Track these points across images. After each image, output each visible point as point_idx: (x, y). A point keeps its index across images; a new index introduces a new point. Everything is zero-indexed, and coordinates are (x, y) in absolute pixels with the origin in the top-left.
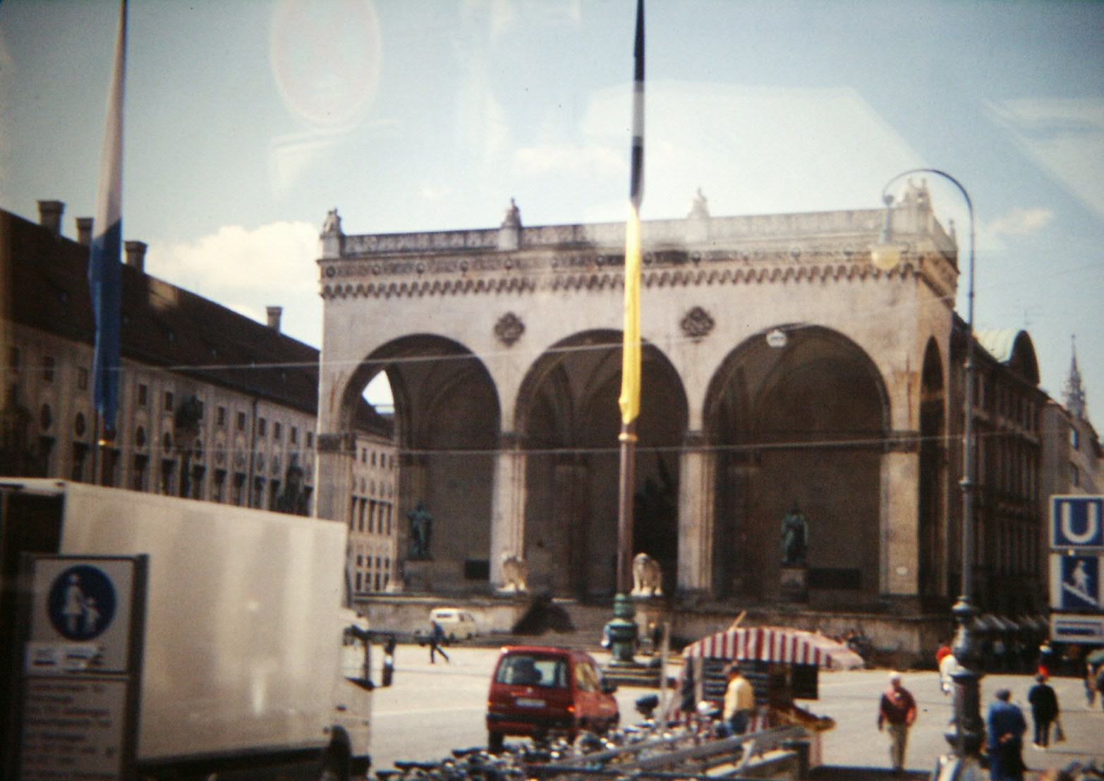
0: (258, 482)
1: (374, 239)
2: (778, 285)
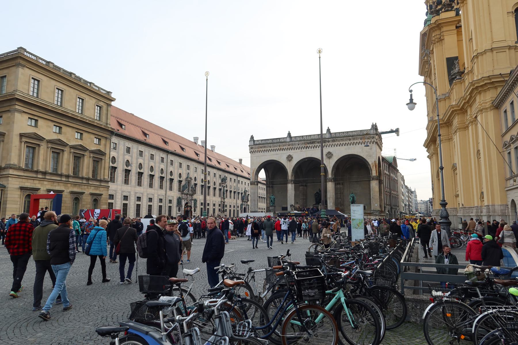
0: (239, 193)
2: (346, 146)
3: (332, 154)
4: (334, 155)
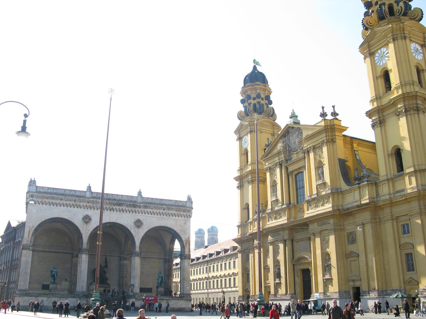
1: (47, 188)
2: (159, 216)
3: (142, 223)
4: (144, 224)
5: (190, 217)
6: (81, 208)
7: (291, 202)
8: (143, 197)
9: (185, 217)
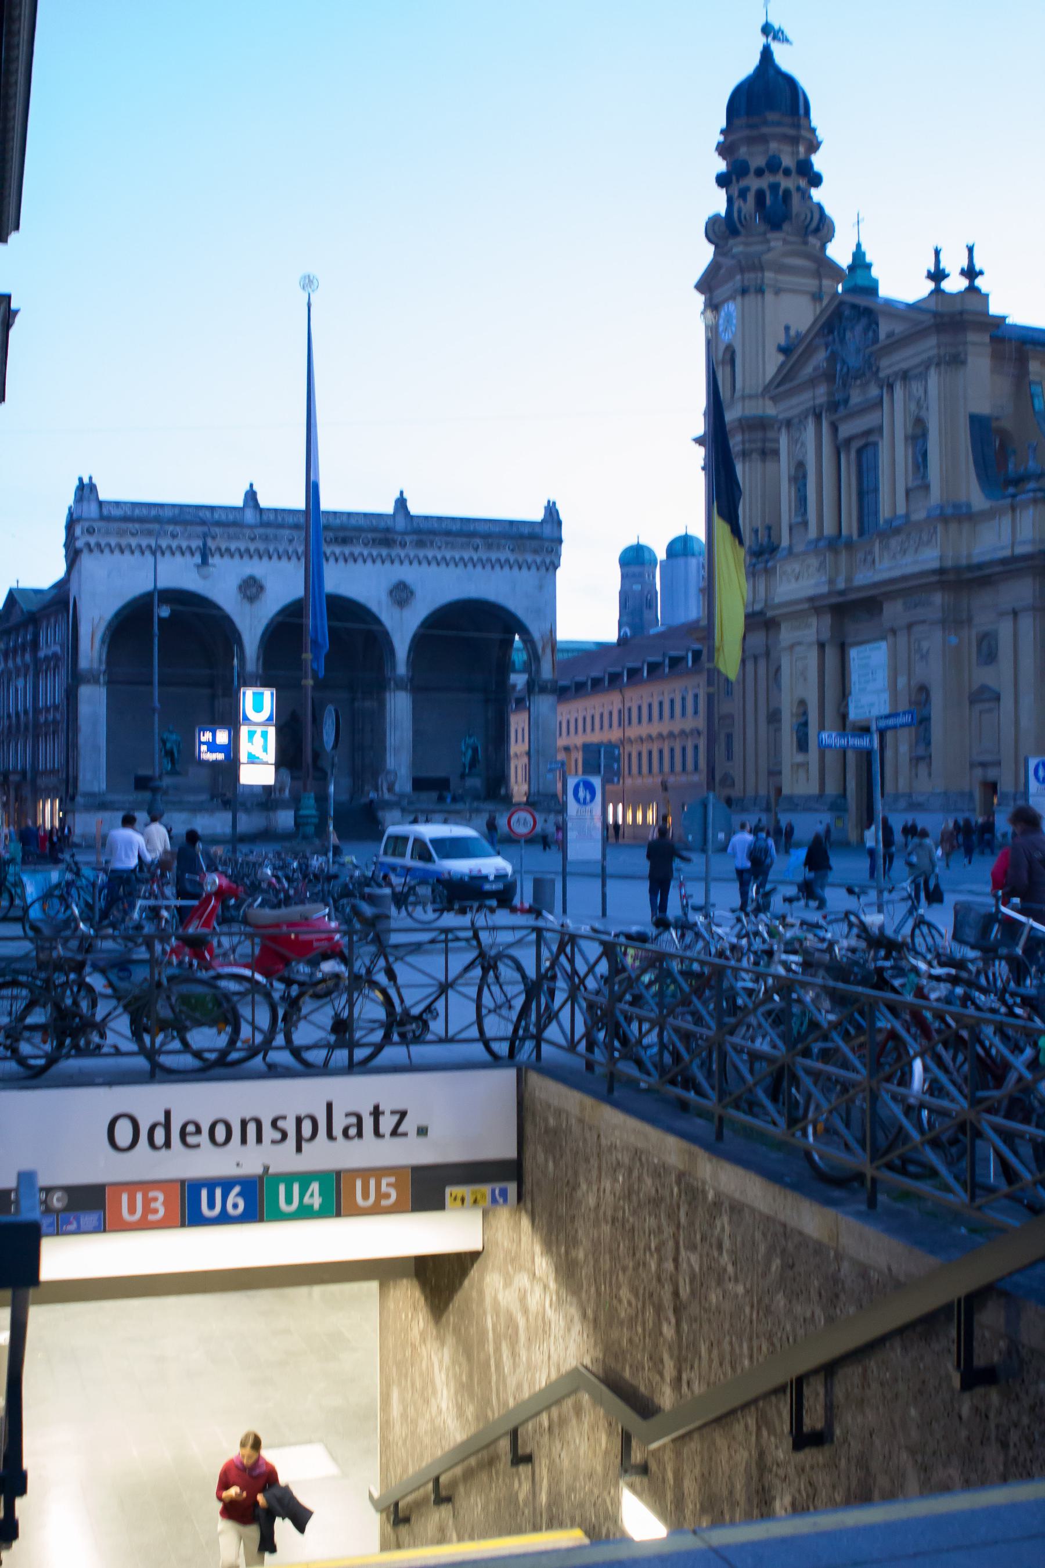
3: (412, 593)
4: (419, 593)
5: (555, 566)
6: (232, 556)
7: (844, 532)
8: (412, 517)
9: (538, 569)
